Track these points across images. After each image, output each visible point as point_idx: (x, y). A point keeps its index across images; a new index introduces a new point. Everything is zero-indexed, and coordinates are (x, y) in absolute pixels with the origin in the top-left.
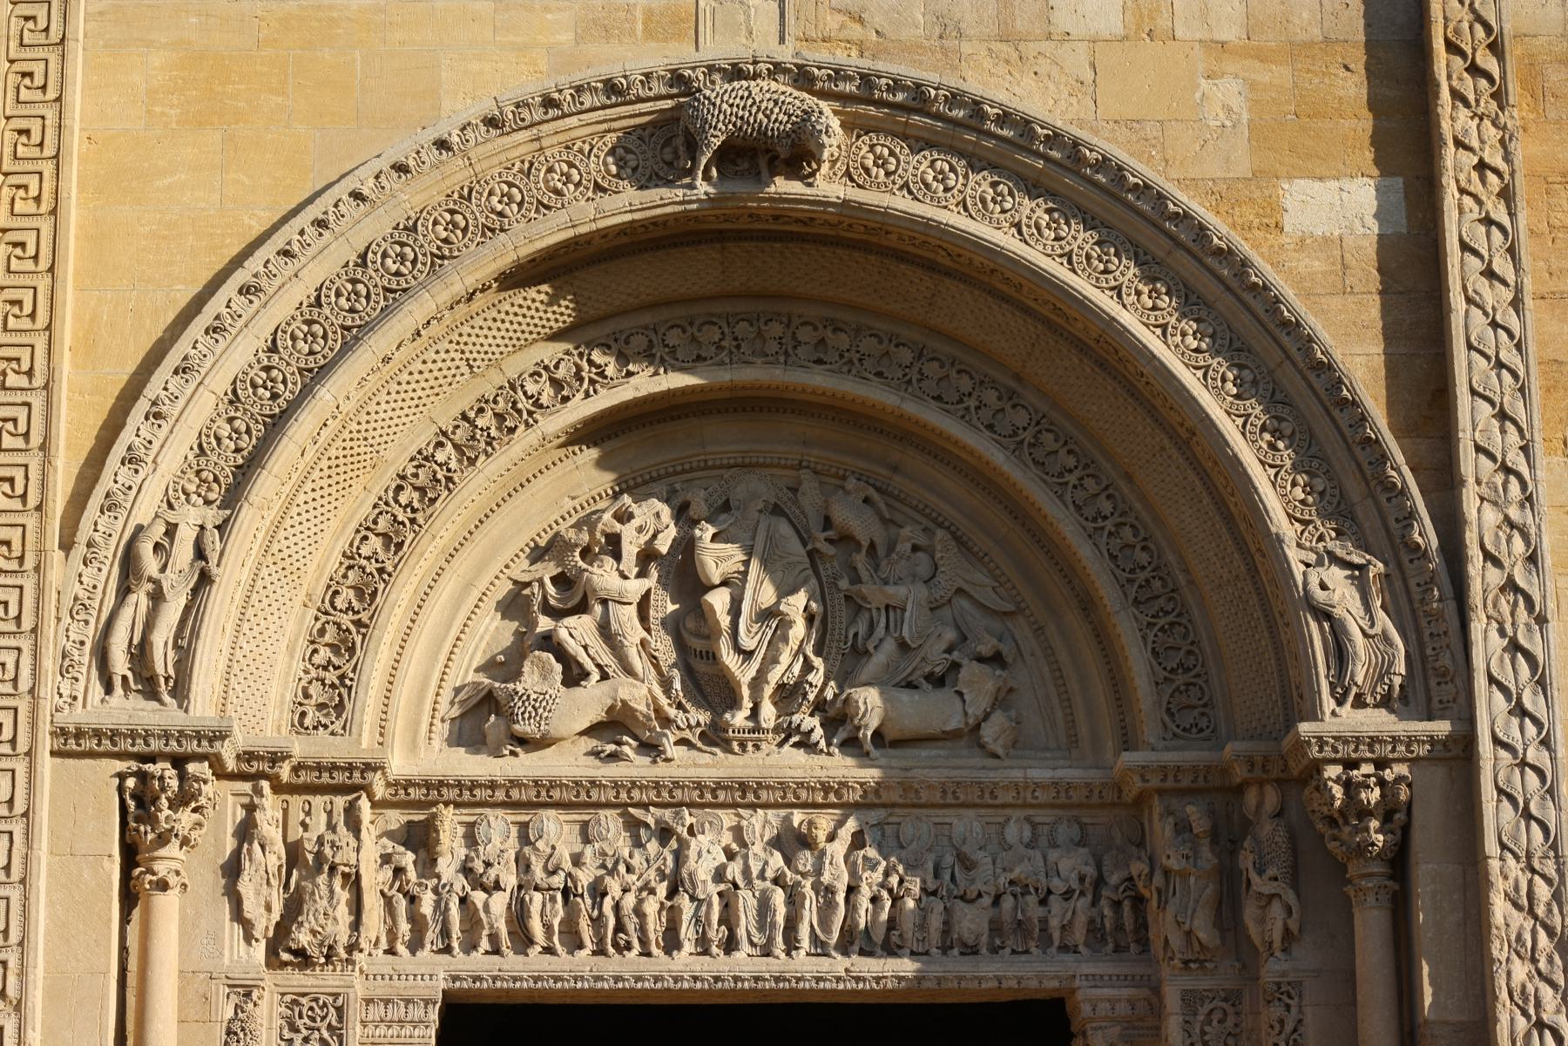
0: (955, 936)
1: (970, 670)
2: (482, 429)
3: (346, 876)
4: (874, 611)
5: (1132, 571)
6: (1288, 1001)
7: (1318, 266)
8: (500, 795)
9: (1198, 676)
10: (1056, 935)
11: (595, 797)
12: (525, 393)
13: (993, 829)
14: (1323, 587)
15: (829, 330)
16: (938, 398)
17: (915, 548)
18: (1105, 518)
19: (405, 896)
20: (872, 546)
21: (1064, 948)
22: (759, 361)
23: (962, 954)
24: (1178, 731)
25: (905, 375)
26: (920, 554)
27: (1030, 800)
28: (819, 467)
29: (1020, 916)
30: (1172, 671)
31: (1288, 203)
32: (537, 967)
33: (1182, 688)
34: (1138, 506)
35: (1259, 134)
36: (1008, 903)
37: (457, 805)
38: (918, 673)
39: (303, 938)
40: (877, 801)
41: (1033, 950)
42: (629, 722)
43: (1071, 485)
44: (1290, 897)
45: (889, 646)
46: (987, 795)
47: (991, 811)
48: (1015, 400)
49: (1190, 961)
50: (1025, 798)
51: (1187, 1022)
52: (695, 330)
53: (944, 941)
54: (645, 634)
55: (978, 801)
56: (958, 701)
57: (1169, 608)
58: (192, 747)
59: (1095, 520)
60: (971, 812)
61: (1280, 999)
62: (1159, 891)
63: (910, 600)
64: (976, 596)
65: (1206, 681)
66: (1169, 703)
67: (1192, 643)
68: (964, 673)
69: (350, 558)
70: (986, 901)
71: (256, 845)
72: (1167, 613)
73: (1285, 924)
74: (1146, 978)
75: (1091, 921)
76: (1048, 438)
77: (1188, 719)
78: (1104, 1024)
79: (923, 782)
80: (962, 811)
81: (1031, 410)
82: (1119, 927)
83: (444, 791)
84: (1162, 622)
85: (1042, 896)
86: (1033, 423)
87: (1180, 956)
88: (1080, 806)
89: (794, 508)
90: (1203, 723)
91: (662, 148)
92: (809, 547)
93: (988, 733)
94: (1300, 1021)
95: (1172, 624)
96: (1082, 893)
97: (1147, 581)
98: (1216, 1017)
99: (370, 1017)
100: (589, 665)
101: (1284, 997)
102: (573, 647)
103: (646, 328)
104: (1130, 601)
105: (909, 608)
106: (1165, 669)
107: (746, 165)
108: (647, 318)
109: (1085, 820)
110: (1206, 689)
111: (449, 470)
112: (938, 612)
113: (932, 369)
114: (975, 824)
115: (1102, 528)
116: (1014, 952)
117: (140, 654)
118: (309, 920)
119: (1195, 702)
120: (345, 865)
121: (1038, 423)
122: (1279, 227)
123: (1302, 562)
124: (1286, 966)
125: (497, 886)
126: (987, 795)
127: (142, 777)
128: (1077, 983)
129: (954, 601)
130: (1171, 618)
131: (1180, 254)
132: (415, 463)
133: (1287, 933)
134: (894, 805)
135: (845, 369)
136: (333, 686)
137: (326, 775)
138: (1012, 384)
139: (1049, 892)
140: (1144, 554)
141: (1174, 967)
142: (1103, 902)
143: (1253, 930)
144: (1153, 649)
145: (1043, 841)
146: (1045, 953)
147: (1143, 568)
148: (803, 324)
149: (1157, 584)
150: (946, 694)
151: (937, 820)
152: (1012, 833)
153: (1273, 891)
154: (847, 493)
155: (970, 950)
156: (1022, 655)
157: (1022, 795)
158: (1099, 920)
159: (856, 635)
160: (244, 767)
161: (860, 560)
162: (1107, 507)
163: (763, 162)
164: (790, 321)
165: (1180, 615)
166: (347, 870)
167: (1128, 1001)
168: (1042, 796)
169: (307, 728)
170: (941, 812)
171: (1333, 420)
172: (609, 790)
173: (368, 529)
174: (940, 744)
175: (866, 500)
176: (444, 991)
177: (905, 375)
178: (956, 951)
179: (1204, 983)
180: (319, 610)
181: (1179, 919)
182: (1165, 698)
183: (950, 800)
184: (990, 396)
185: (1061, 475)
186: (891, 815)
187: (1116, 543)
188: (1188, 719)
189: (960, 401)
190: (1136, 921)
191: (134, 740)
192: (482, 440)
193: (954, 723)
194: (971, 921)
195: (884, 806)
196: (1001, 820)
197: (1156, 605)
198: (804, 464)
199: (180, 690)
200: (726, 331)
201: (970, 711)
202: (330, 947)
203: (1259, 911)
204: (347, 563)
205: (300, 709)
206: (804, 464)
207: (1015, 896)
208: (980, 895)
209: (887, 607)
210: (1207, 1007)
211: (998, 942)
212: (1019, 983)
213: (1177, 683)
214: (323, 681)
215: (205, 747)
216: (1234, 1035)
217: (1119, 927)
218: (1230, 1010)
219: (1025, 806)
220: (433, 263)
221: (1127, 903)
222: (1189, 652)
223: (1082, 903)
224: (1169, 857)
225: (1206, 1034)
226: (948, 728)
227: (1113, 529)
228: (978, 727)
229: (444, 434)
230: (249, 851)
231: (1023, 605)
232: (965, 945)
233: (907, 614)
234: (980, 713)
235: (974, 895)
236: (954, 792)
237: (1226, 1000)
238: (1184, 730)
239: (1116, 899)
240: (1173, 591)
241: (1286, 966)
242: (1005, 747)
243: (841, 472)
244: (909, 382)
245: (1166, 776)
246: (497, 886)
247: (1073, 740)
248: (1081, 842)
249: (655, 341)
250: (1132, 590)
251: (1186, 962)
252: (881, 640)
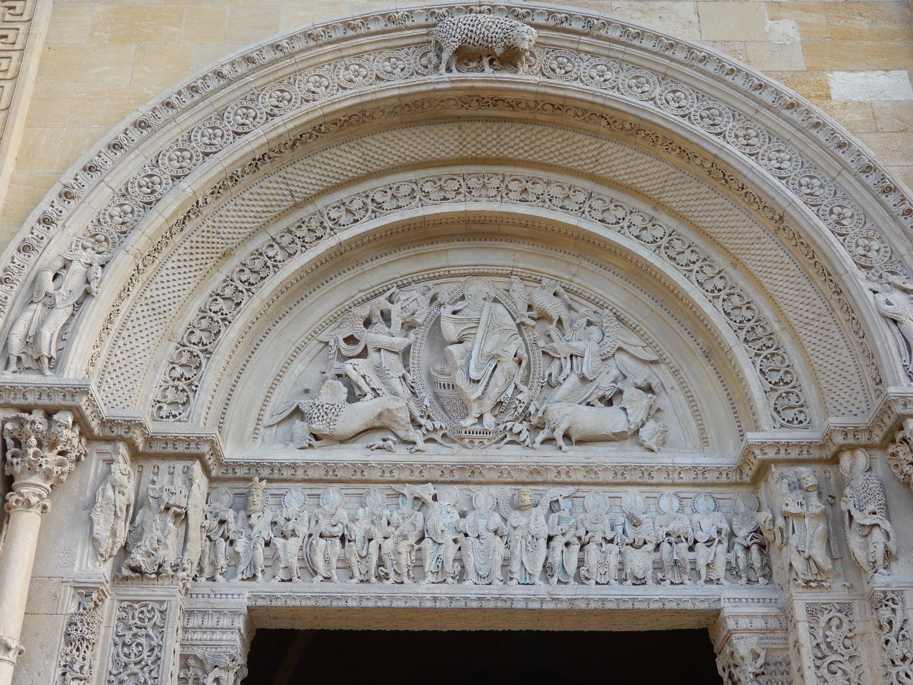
0: (629, 571)
1: (630, 392)
2: (299, 238)
3: (177, 515)
4: (562, 360)
5: (741, 322)
6: (894, 606)
7: (857, 117)
8: (300, 474)
9: (794, 387)
10: (703, 571)
11: (367, 475)
12: (329, 218)
13: (651, 501)
14: (889, 303)
15: (530, 184)
16: (602, 221)
17: (589, 323)
18: (720, 290)
19: (226, 541)
20: (560, 321)
21: (709, 581)
22: (484, 200)
23: (633, 584)
24: (785, 423)
25: (580, 208)
26: (592, 327)
27: (677, 480)
28: (524, 275)
29: (675, 557)
30: (776, 384)
31: (832, 84)
32: (318, 590)
33: (784, 395)
34: (742, 283)
35: (808, 48)
36: (665, 547)
37: (269, 481)
38: (594, 396)
39: (138, 557)
40: (568, 480)
41: (686, 581)
42: (393, 425)
43: (694, 271)
44: (886, 525)
45: (574, 379)
46: (646, 476)
47: (648, 488)
48: (653, 222)
49: (810, 581)
50: (673, 479)
51: (812, 628)
52: (442, 183)
53: (620, 576)
54: (404, 372)
55: (640, 481)
56: (622, 413)
57: (769, 344)
58: (58, 400)
59: (712, 291)
60: (635, 490)
61: (886, 605)
62: (781, 530)
63: (587, 350)
64: (632, 352)
65: (801, 391)
66: (775, 404)
67: (788, 366)
68: (625, 396)
69: (203, 312)
70: (650, 547)
71: (109, 487)
72: (768, 347)
73: (886, 546)
74: (773, 601)
75: (729, 563)
76: (677, 244)
77: (790, 415)
78: (745, 635)
79: (600, 466)
80: (629, 488)
81: (665, 227)
82: (750, 567)
83: (261, 471)
84: (765, 353)
85: (691, 544)
86: (667, 235)
87: (803, 577)
88: (712, 485)
89: (507, 300)
90: (801, 417)
91: (421, 58)
92: (518, 321)
93: (644, 433)
94: (905, 621)
95: (773, 355)
96: (720, 542)
97: (753, 328)
98: (835, 622)
99: (191, 625)
100: (366, 389)
101: (890, 603)
102: (354, 375)
103: (411, 181)
104: (742, 340)
105: (586, 355)
106: (770, 383)
107: (475, 64)
108: (411, 176)
109: (716, 496)
110: (801, 396)
111: (275, 261)
112: (606, 362)
113: (598, 205)
114: (638, 498)
115: (718, 297)
116: (672, 583)
117: (33, 340)
118: (146, 544)
119: (793, 403)
120: (178, 507)
121: (670, 235)
122: (828, 97)
123: (871, 290)
124: (888, 579)
125: (294, 534)
126: (646, 476)
127: (21, 422)
128: (723, 604)
129: (617, 356)
130: (771, 351)
131: (764, 111)
132: (254, 257)
133: (887, 553)
134: (580, 484)
135: (541, 204)
136: (183, 391)
137: (170, 445)
138: (653, 213)
139: (696, 542)
140: (749, 311)
141: (799, 586)
142: (737, 547)
143: (860, 555)
144: (761, 370)
145: (688, 510)
146: (696, 584)
147: (749, 320)
148: (514, 180)
149: (759, 330)
150: (615, 408)
151: (611, 495)
152: (665, 503)
153: (873, 522)
154: (543, 288)
155: (640, 581)
156: (665, 389)
158: (734, 562)
159: (550, 375)
160: (107, 432)
161: (552, 328)
162: (720, 284)
163: (486, 61)
164: (504, 178)
165: (777, 349)
166: (178, 510)
167: (763, 616)
168: (687, 477)
169: (162, 417)
170: (614, 489)
171: (882, 204)
172: (376, 470)
173: (218, 295)
174: (611, 443)
175: (555, 294)
176: (248, 607)
177: (580, 208)
178: (629, 582)
179: (821, 597)
180: (179, 343)
181: (800, 549)
182: (772, 406)
183: (619, 479)
184: (637, 220)
185: (687, 265)
186: (578, 491)
187: (728, 307)
188: (790, 415)
189: (618, 223)
190: (762, 560)
191: (15, 394)
192: (299, 244)
193: (621, 427)
194: (640, 561)
195: (573, 484)
196: (657, 495)
197: (759, 344)
198: (514, 273)
199: (55, 364)
200: (462, 183)
201: (631, 419)
202: (160, 566)
203: (862, 540)
204: (201, 315)
205: (158, 405)
206: (514, 273)
207: (671, 544)
208: (645, 543)
209: (571, 356)
210: (826, 617)
211: (660, 576)
212: (678, 604)
213: (780, 392)
214: (177, 388)
215: (69, 402)
216: (850, 638)
217: (750, 567)
218: (845, 620)
219: (673, 485)
220: (267, 119)
221: (754, 548)
222: (787, 372)
223: (721, 549)
224: (787, 505)
225: (828, 637)
226: (617, 431)
227: (726, 297)
228: (637, 431)
229: (274, 239)
230: (104, 490)
231: (664, 356)
232: (637, 579)
233: (585, 359)
234: (638, 421)
235: (641, 543)
236: (623, 474)
237: (839, 611)
238: (788, 422)
239: (746, 545)
240: (771, 334)
241: (888, 579)
242: (657, 444)
243: (539, 278)
244: (583, 212)
245: (779, 450)
246: (294, 534)
247: (705, 441)
248: (717, 508)
249: (416, 188)
250: (743, 334)
251: (807, 582)
252: (568, 376)
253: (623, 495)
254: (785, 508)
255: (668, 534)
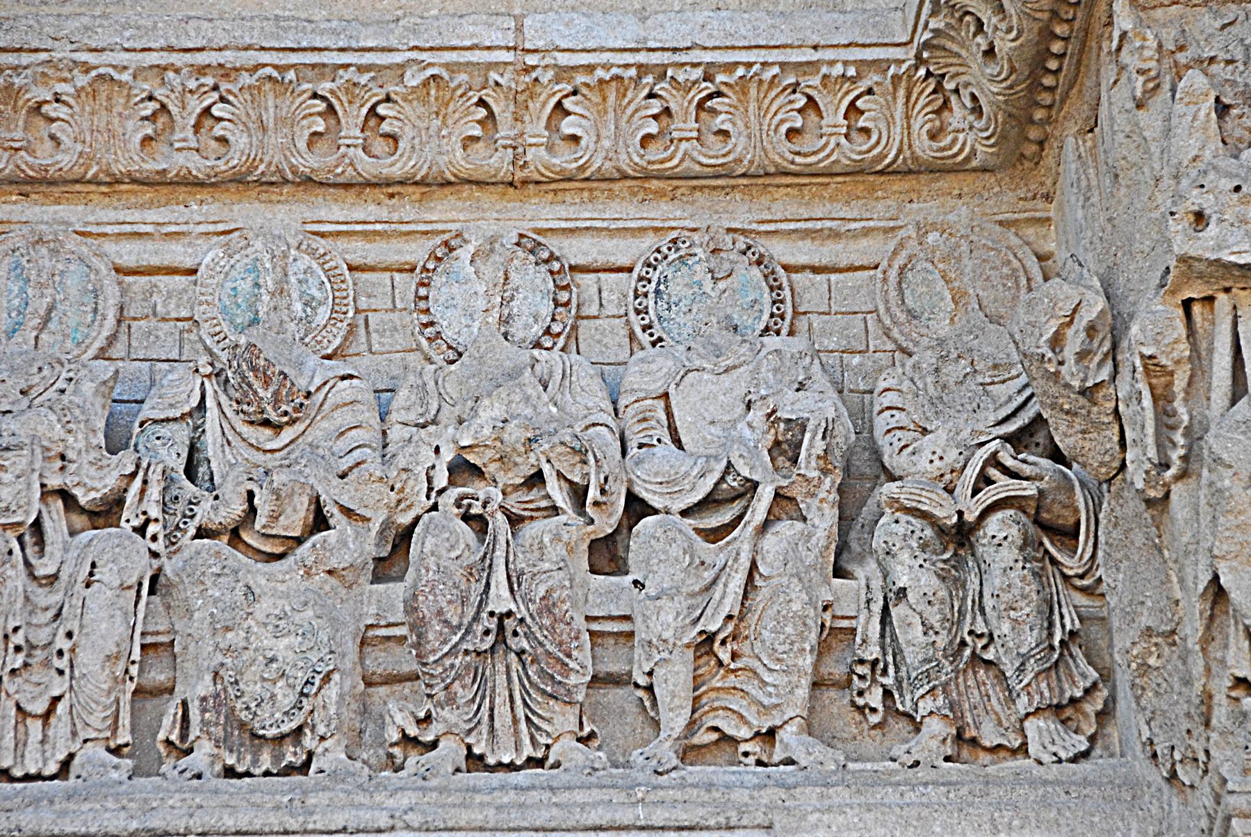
23: (230, 772)
29: (501, 600)
41: (566, 748)
46: (351, 129)
47: (368, 210)
55: (308, 162)
85: (606, 524)
109: (782, 251)
126: (351, 129)
139: (637, 508)
151: (129, 254)
157: (505, 131)
190: (1048, 609)
196: (416, 252)
207: (478, 523)
208: (320, 522)
235: (295, 519)
239: (946, 514)
253: (209, 256)
254: (1183, 241)
255: (463, 469)
